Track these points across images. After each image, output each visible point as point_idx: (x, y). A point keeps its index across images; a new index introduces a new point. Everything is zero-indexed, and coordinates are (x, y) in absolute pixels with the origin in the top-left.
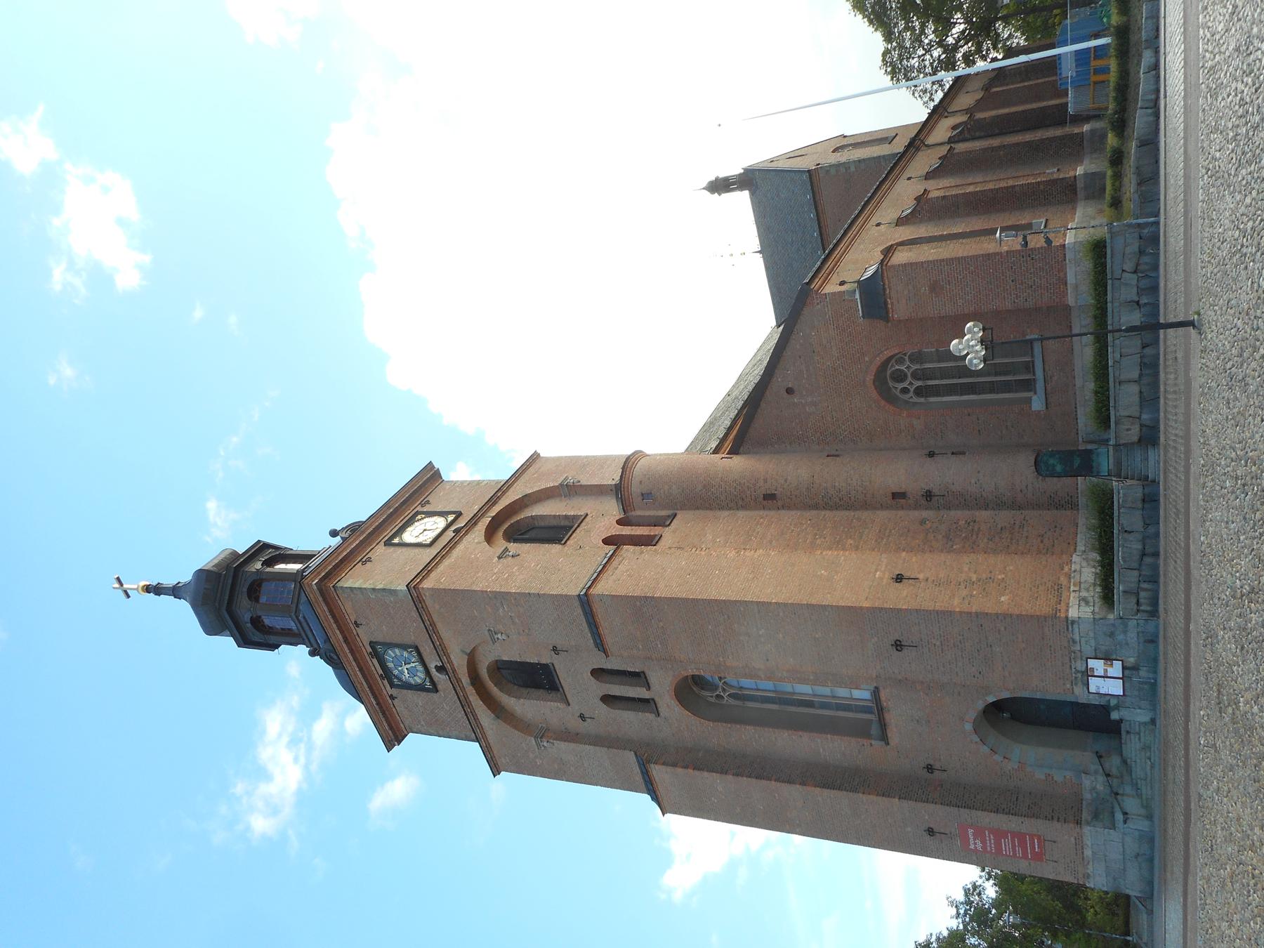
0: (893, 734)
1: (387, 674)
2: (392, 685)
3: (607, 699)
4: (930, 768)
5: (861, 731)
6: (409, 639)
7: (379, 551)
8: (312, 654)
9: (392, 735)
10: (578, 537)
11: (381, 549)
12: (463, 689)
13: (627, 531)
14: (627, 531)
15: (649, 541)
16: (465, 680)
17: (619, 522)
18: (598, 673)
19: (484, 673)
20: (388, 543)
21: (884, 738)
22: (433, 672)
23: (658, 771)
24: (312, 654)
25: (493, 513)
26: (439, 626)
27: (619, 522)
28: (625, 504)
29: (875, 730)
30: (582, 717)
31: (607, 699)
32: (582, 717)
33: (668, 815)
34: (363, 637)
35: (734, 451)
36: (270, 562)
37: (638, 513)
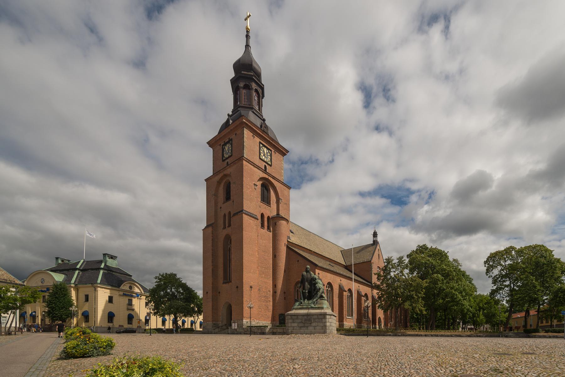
0: (224, 285)
1: (225, 144)
2: (223, 145)
3: (225, 215)
4: (219, 293)
6: (234, 154)
7: (258, 140)
9: (211, 143)
10: (264, 206)
13: (266, 219)
14: (266, 219)
15: (262, 226)
17: (268, 217)
18: (230, 213)
21: (224, 283)
22: (227, 161)
25: (270, 178)
27: (268, 217)
28: (273, 218)
35: (288, 247)
36: (256, 91)
37: (271, 222)
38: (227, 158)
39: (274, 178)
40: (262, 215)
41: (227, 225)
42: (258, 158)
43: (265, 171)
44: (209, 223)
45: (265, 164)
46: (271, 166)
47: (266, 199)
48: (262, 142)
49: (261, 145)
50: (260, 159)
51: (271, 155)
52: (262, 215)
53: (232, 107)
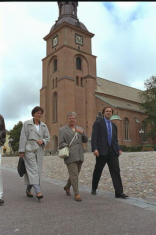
0: (53, 124)
1: (54, 38)
2: (53, 39)
3: (54, 80)
5: (53, 120)
7: (74, 33)
8: (56, 21)
11: (74, 33)
12: (52, 54)
13: (80, 79)
16: (54, 55)
17: (82, 78)
19: (55, 58)
20: (76, 34)
23: (45, 89)
24: (56, 21)
26: (60, 50)
29: (54, 122)
30: (51, 76)
31: (54, 80)
32: (51, 76)
33: (90, 30)
34: (59, 33)
38: (55, 46)
39: (84, 53)
40: (77, 77)
41: (55, 87)
42: (74, 43)
43: (79, 50)
44: (44, 86)
45: (78, 45)
46: (83, 46)
47: (79, 67)
48: (77, 33)
49: (76, 35)
50: (76, 43)
51: (82, 40)
52: (77, 77)
53: (58, 16)
